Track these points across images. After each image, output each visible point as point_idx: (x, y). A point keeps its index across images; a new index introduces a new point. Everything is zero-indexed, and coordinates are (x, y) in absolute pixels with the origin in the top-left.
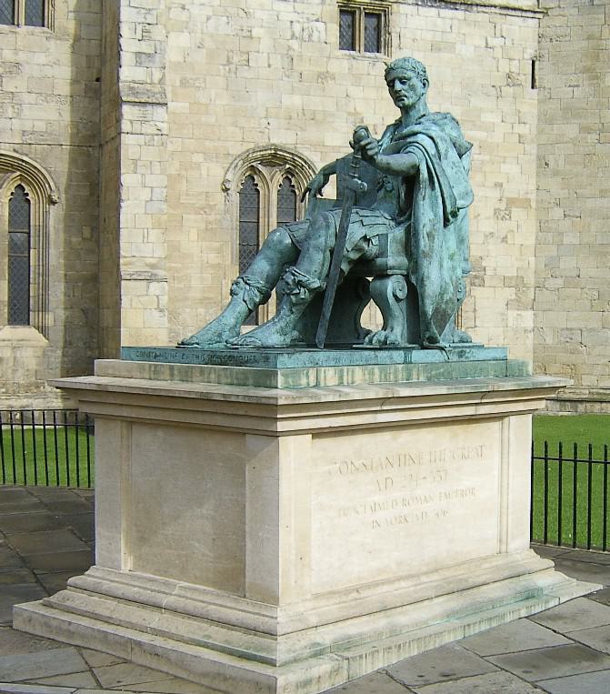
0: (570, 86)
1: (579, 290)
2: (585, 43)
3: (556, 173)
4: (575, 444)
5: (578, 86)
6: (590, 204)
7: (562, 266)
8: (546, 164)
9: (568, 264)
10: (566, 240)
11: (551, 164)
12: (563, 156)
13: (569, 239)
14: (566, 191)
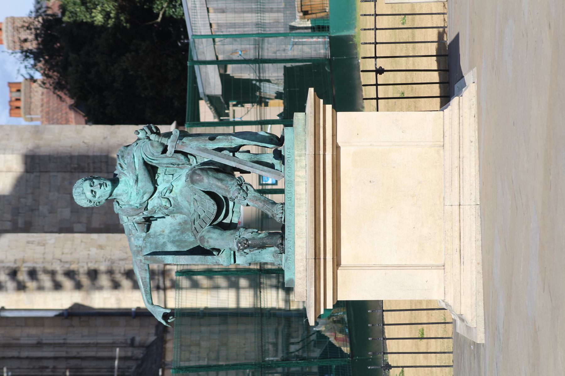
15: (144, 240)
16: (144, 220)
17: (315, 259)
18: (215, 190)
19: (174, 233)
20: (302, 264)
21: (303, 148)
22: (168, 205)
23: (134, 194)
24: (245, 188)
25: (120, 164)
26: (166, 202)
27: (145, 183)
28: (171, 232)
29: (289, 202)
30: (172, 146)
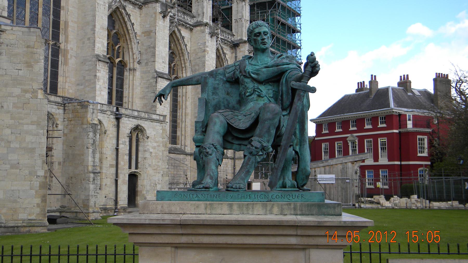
0: (16, 69)
1: (19, 170)
2: (25, 49)
3: (8, 112)
4: (125, 246)
5: (21, 70)
6: (26, 127)
7: (9, 158)
8: (2, 107)
9: (13, 157)
10: (12, 146)
11: (5, 107)
12: (12, 104)
13: (12, 146)
14: (13, 121)
15: (221, 79)
16: (236, 77)
17: (180, 224)
18: (259, 126)
19: (226, 103)
20: (178, 209)
21: (304, 212)
22: (248, 94)
23: (257, 67)
24: (261, 153)
25: (282, 55)
26: (250, 92)
27: (265, 74)
28: (227, 100)
29: (246, 196)
30: (300, 86)
